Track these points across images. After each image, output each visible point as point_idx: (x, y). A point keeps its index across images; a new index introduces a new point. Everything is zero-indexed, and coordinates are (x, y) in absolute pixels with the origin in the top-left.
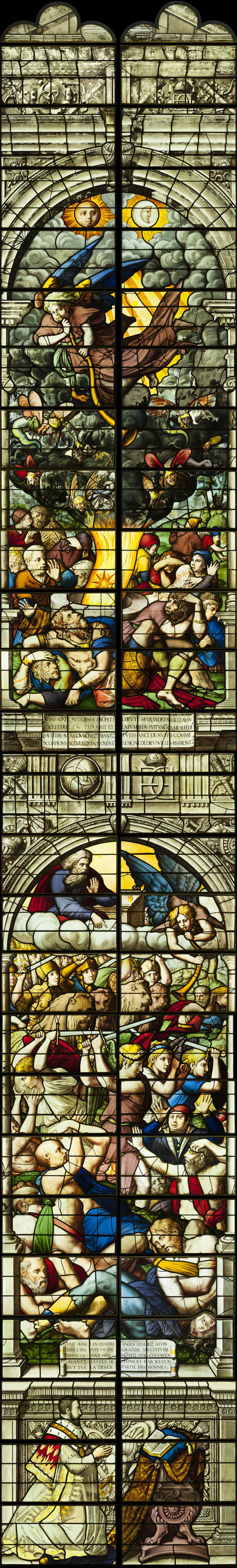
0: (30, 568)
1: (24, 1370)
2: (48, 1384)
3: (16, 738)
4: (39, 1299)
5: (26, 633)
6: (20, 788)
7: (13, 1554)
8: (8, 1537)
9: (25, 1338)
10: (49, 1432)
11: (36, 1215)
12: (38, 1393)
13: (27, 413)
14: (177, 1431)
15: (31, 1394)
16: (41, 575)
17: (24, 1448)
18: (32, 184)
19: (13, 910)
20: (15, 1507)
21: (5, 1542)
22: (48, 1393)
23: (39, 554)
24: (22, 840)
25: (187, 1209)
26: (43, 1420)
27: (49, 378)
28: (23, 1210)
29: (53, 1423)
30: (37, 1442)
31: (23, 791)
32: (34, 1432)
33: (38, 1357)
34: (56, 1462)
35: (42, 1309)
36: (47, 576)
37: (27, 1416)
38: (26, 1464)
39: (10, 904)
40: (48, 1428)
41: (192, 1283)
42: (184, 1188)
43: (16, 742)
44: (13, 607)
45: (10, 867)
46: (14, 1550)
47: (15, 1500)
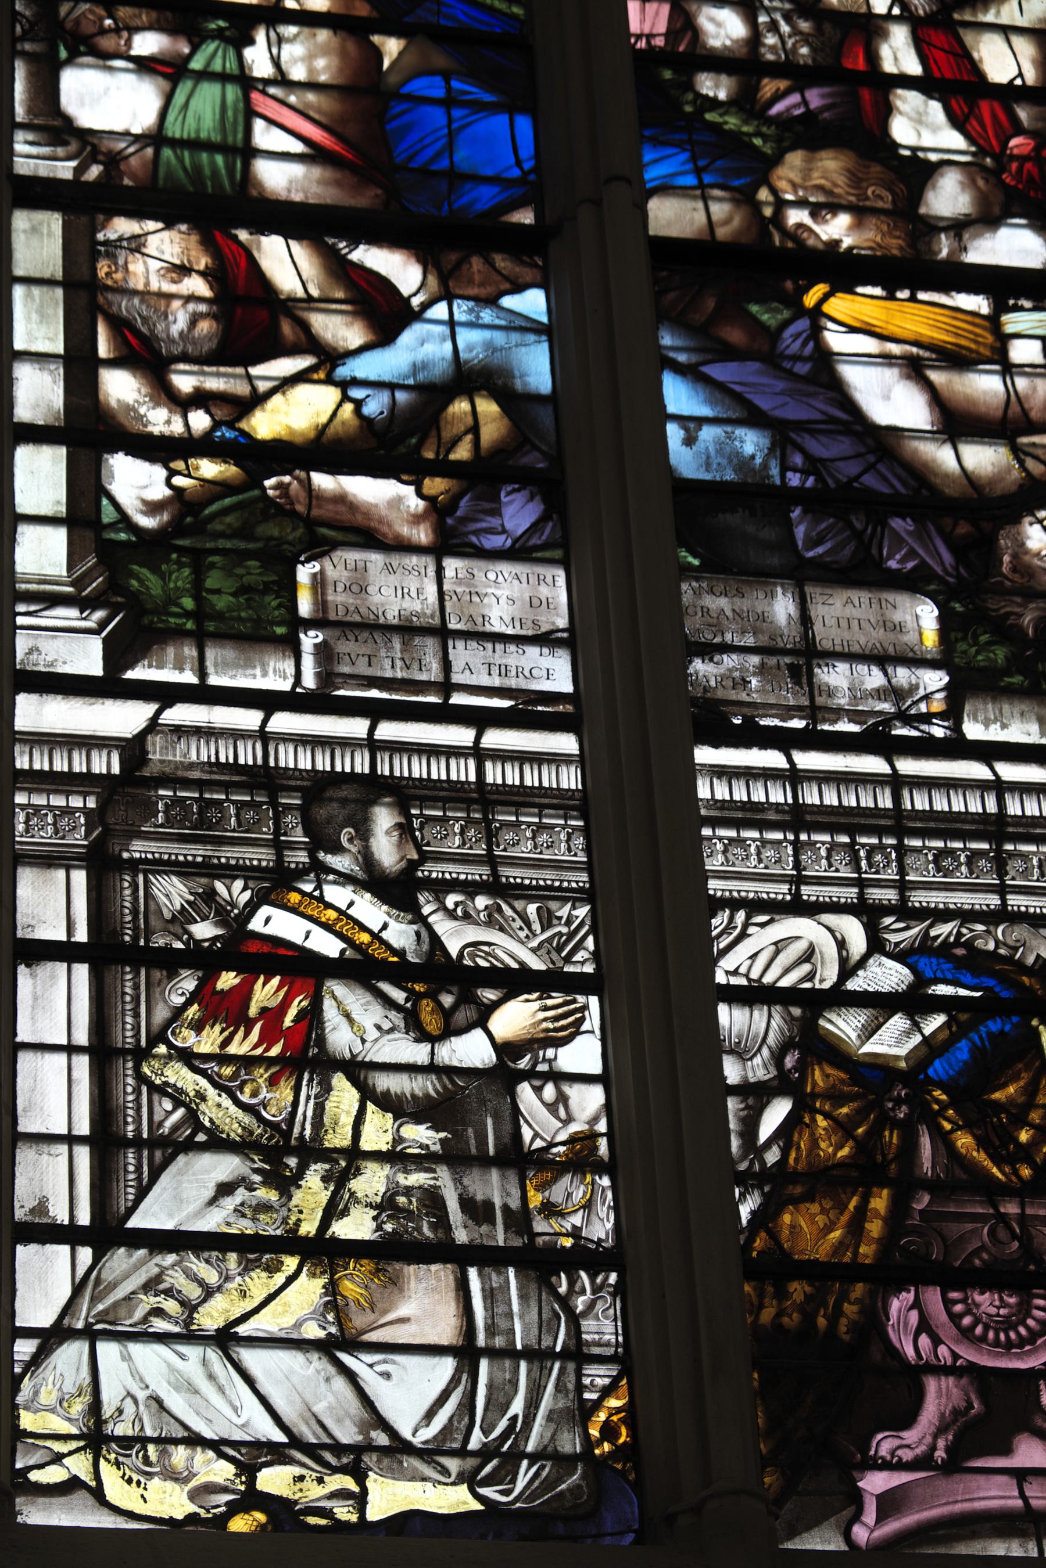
1: (118, 654)
2: (249, 719)
4: (184, 382)
7: (73, 1484)
8: (48, 1396)
9: (124, 519)
10: (256, 924)
11: (166, 70)
12: (199, 752)
14: (969, 961)
15: (157, 750)
17: (127, 982)
20: (85, 1255)
21: (27, 1421)
22: (247, 754)
25: (920, 125)
26: (229, 872)
28: (107, 43)
29: (275, 885)
30: (205, 960)
32: (183, 918)
33: (188, 603)
34: (308, 1057)
35: (200, 421)
37: (138, 849)
38: (141, 1055)
40: (252, 907)
41: (985, 386)
42: (899, 54)
46: (79, 1466)
47: (84, 1218)
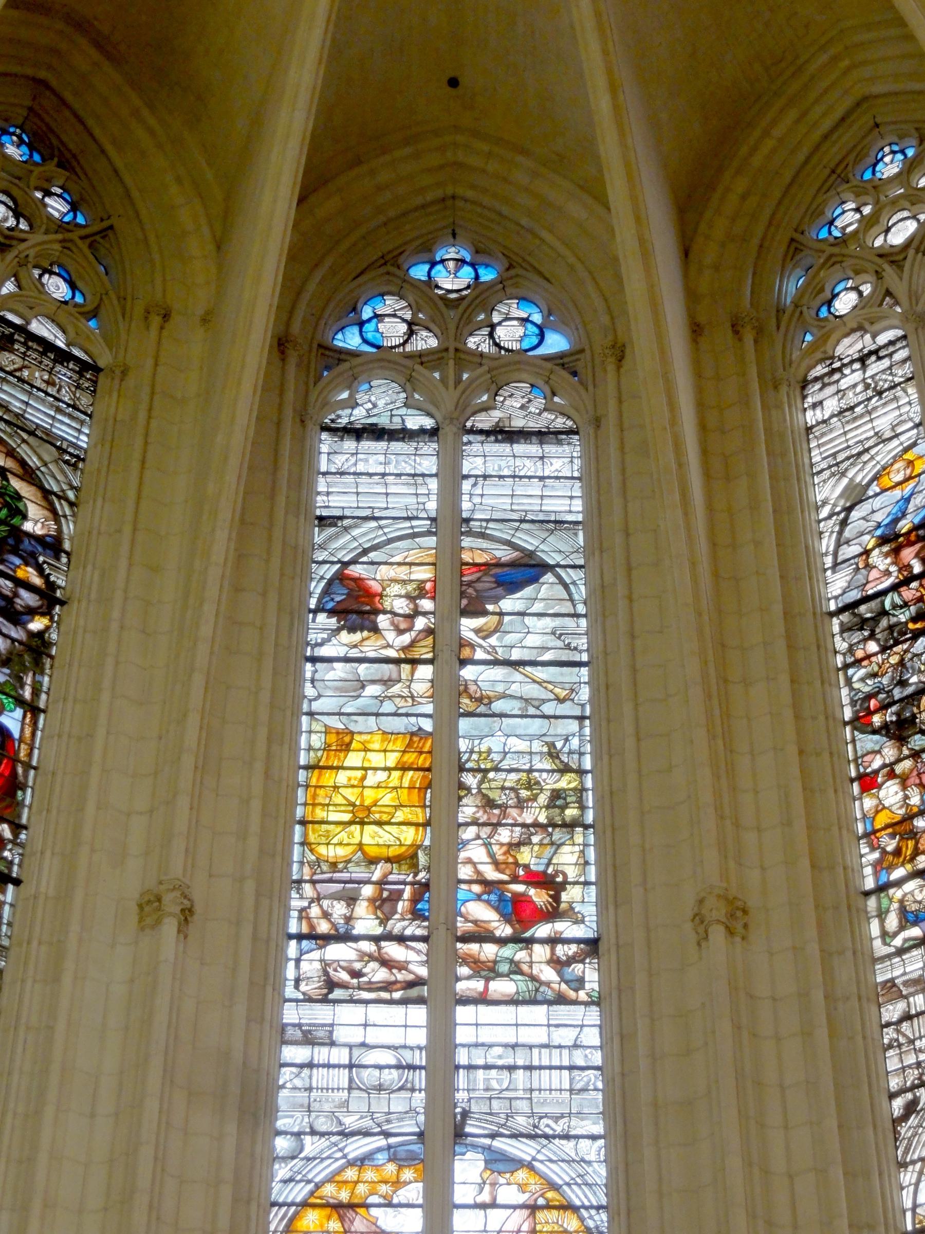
0: (887, 805)
3: (894, 985)
5: (891, 868)
6: (904, 1035)
13: (865, 663)
16: (901, 807)
18: (843, 474)
19: (913, 1181)
23: (896, 788)
24: (915, 1095)
27: (884, 623)
31: (907, 1037)
36: (908, 805)
39: (909, 1174)
43: (894, 989)
44: (873, 849)
45: (903, 1132)
